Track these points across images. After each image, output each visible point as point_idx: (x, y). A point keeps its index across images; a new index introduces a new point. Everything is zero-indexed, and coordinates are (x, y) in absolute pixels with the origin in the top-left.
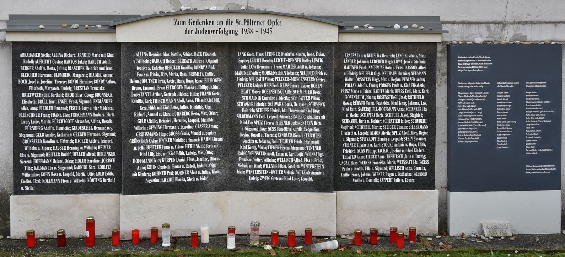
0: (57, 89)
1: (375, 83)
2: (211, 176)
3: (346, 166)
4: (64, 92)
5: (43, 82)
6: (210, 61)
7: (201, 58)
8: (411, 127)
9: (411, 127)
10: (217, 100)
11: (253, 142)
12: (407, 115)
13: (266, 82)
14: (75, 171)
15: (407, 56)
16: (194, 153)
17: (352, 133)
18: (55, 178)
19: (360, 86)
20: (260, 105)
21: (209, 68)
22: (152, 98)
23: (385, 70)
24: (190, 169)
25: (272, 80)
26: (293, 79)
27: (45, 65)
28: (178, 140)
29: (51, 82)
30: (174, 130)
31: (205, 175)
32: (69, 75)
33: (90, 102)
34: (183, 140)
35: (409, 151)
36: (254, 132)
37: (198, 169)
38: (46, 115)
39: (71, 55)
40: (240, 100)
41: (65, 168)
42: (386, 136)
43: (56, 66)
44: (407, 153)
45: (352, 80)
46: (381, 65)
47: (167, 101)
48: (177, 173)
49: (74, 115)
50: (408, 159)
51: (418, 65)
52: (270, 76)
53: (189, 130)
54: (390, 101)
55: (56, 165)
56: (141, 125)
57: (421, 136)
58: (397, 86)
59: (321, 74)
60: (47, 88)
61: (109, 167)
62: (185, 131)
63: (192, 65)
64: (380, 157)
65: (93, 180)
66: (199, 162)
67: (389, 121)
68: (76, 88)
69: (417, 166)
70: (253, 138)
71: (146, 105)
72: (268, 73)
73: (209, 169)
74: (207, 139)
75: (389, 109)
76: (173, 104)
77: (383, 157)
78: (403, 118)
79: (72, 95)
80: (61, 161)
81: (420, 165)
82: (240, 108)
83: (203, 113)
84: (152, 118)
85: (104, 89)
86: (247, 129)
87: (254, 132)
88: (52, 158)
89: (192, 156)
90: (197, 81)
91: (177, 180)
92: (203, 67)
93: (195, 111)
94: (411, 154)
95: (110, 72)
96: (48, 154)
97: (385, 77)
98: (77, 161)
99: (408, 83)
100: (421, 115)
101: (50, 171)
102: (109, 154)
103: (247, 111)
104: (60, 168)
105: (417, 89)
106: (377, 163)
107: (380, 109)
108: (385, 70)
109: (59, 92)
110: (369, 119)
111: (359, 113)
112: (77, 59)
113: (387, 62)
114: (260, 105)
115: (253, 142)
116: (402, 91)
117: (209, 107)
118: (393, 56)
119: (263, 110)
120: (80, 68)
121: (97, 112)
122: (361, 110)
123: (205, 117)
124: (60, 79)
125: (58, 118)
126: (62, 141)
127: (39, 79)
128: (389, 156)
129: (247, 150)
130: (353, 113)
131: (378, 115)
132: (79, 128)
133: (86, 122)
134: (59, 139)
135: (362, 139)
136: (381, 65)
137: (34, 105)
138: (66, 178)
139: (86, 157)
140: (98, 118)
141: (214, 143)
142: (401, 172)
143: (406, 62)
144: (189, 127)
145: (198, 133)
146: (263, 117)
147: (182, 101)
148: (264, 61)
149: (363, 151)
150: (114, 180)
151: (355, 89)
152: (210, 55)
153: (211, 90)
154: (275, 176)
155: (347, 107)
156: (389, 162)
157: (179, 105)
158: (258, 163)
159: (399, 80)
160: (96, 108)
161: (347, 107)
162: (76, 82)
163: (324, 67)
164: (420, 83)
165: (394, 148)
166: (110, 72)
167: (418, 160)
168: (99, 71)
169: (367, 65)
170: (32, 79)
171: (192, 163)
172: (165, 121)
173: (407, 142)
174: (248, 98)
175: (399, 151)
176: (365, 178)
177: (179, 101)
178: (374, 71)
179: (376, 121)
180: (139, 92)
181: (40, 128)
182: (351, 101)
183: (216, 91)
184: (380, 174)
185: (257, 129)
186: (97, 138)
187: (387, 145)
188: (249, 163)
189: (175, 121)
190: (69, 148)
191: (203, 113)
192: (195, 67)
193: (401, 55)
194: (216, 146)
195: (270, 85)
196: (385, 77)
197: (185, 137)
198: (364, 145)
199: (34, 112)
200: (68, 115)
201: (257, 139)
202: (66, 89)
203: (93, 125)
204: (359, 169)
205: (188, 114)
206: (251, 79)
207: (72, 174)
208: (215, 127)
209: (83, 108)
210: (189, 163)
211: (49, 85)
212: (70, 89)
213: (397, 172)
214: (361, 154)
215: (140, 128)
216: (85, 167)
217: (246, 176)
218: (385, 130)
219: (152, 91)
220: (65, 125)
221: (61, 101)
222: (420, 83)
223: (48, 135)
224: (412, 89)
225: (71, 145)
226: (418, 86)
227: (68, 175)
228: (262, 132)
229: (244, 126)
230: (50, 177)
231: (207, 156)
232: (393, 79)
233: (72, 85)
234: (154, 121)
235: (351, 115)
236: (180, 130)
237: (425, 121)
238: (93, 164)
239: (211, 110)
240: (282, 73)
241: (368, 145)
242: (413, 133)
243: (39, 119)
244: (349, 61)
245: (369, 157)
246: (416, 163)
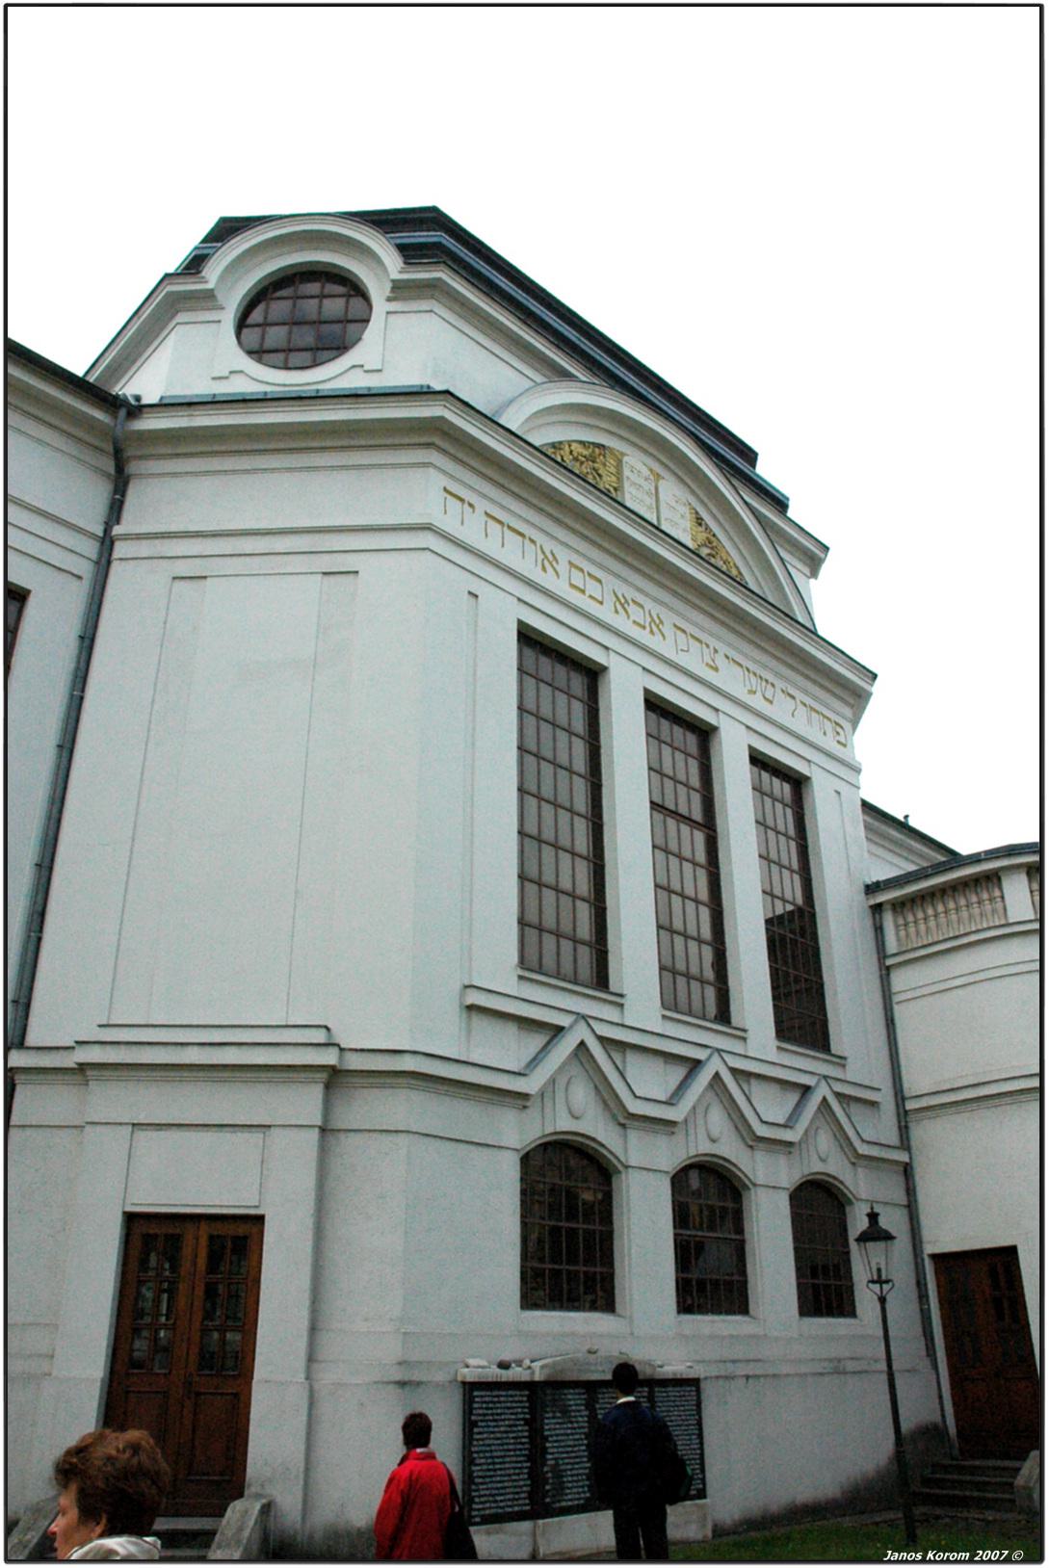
112: (506, 1396)
233: (504, 1420)
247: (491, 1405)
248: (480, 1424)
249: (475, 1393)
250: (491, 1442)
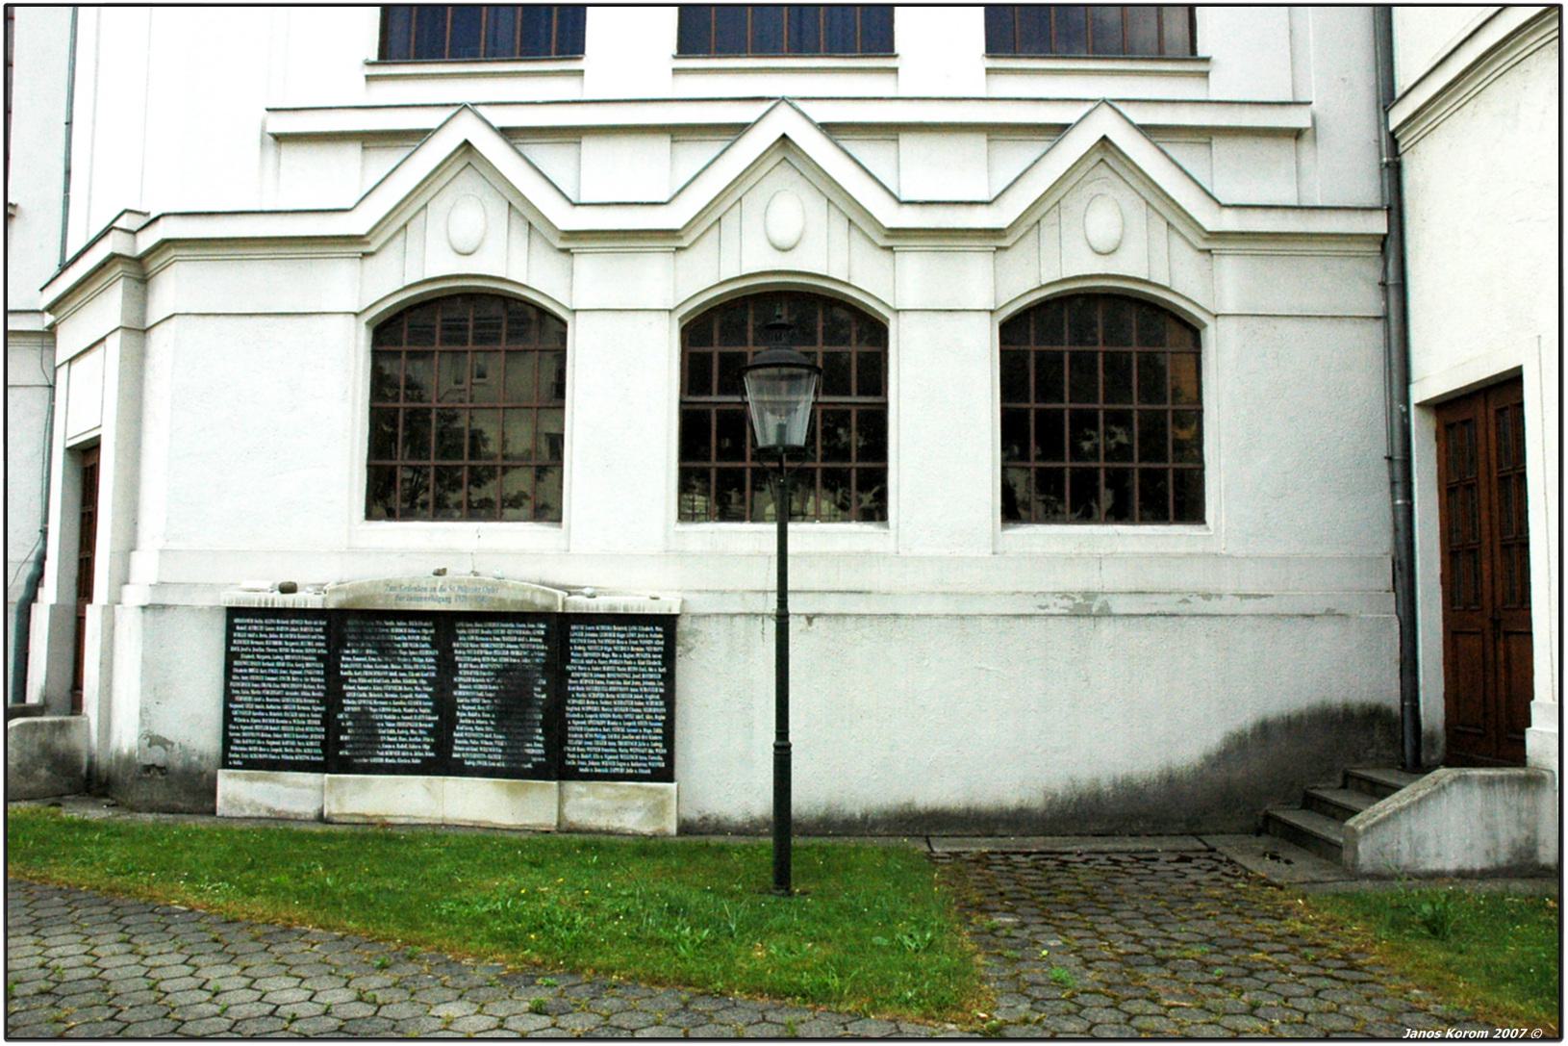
0: (269, 657)
1: (604, 659)
3: (571, 753)
4: (276, 661)
5: (254, 650)
6: (425, 631)
7: (415, 628)
8: (645, 710)
9: (645, 710)
10: (433, 674)
11: (469, 722)
12: (641, 697)
13: (484, 655)
14: (283, 747)
15: (643, 629)
16: (407, 732)
17: (578, 716)
18: (262, 753)
19: (588, 662)
20: (478, 680)
21: (425, 638)
22: (362, 670)
23: (616, 645)
24: (402, 750)
25: (490, 653)
26: (513, 653)
27: (257, 632)
28: (389, 717)
29: (262, 650)
30: (385, 706)
31: (419, 758)
32: (280, 643)
33: (300, 672)
34: (394, 717)
35: (643, 737)
36: (471, 711)
37: (409, 750)
38: (256, 685)
39: (283, 622)
40: (458, 675)
41: (273, 743)
42: (618, 720)
43: (268, 633)
44: (641, 740)
45: (578, 655)
46: (613, 638)
47: (379, 673)
48: (387, 753)
49: (284, 686)
50: (642, 747)
51: (655, 639)
52: (489, 649)
53: (401, 707)
54: (621, 680)
55: (265, 739)
56: (350, 699)
57: (657, 721)
58: (630, 663)
59: (543, 647)
60: (258, 657)
61: (318, 744)
62: (397, 707)
63: (406, 635)
64: (610, 744)
65: (301, 758)
66: (411, 743)
67: (621, 703)
68: (287, 657)
69: (652, 755)
70: (471, 718)
71: (356, 677)
72: (487, 646)
73: (423, 751)
74: (420, 717)
75: (621, 689)
76: (385, 677)
77: (614, 744)
78: (637, 700)
79: (283, 665)
80: (269, 736)
81: (656, 754)
83: (417, 688)
84: (361, 692)
85: (314, 659)
86: (464, 707)
87: (471, 711)
88: (260, 731)
89: (403, 736)
90: (412, 653)
91: (387, 760)
92: (418, 638)
93: (408, 685)
94: (646, 741)
95: (322, 641)
96: (257, 727)
97: (616, 652)
98: (285, 735)
99: (642, 659)
100: (658, 697)
101: (258, 746)
102: (318, 729)
103: (465, 687)
104: (268, 742)
105: (653, 667)
106: (606, 750)
107: (611, 689)
108: (616, 645)
109: (270, 661)
110: (598, 699)
112: (290, 626)
113: (618, 635)
114: (478, 680)
115: (469, 722)
116: (635, 669)
117: (423, 682)
118: (625, 629)
119: (481, 687)
120: (291, 636)
121: (307, 683)
122: (588, 689)
123: (419, 693)
124: (272, 647)
125: (269, 689)
126: (271, 714)
127: (251, 646)
128: (620, 743)
129: (464, 731)
130: (580, 692)
131: (608, 696)
132: (288, 700)
133: (296, 693)
134: (268, 711)
135: (590, 722)
136: (613, 638)
137: (245, 674)
138: (274, 753)
139: (295, 732)
140: (310, 691)
141: (428, 722)
142: (634, 761)
143: (639, 636)
144: (402, 703)
145: (411, 711)
146: (481, 694)
147: (395, 674)
148: (483, 632)
149: (591, 736)
150: (322, 759)
151: (582, 665)
152: (426, 624)
153: (426, 664)
154: (492, 761)
155: (573, 685)
156: (620, 750)
157: (390, 678)
158: (475, 746)
159: (632, 656)
160: (307, 680)
161: (573, 685)
162: (287, 650)
163: (546, 639)
164: (657, 660)
165: (626, 734)
166: (322, 641)
167: (654, 748)
168: (311, 640)
169: (596, 638)
170: (244, 646)
171: (404, 743)
172: (375, 695)
173: (642, 727)
174: (466, 673)
175: (632, 737)
176: (593, 767)
177: (391, 674)
178: (604, 645)
179: (606, 703)
180: (349, 663)
181: (250, 699)
182: (578, 679)
183: (431, 664)
184: (610, 764)
185: (474, 708)
186: (306, 712)
187: (618, 730)
188: (465, 746)
189: (387, 696)
190: (278, 721)
191: (417, 688)
192: (409, 638)
193: (635, 628)
194: (431, 725)
195: (488, 659)
196: (617, 652)
197: (397, 714)
198: (592, 729)
199: (244, 681)
200: (278, 686)
201: (474, 719)
202: (278, 657)
203: (303, 697)
204: (586, 757)
205: (400, 688)
206: (469, 652)
207: (280, 750)
208: (431, 704)
209: (294, 679)
210: (401, 743)
211: (262, 654)
212: (281, 658)
213: (629, 761)
214: (588, 740)
215: (348, 702)
216: (293, 743)
217: (462, 760)
218: (617, 713)
219: (362, 663)
220: (275, 696)
221: (272, 671)
222: (657, 660)
223: (258, 707)
224: (647, 666)
225: (280, 718)
226: (655, 663)
227: (276, 750)
228: (480, 712)
229: (461, 704)
230: (258, 752)
232: (625, 656)
233: (283, 654)
234: (364, 695)
235: (578, 695)
236: (392, 706)
237: (661, 703)
238: (301, 740)
239: (426, 685)
240: (502, 645)
241: (597, 729)
242: (648, 717)
243: (249, 689)
244: (576, 634)
245: (597, 743)
246: (651, 751)
247: (261, 636)
248: (242, 656)
249: (237, 621)
250: (262, 678)
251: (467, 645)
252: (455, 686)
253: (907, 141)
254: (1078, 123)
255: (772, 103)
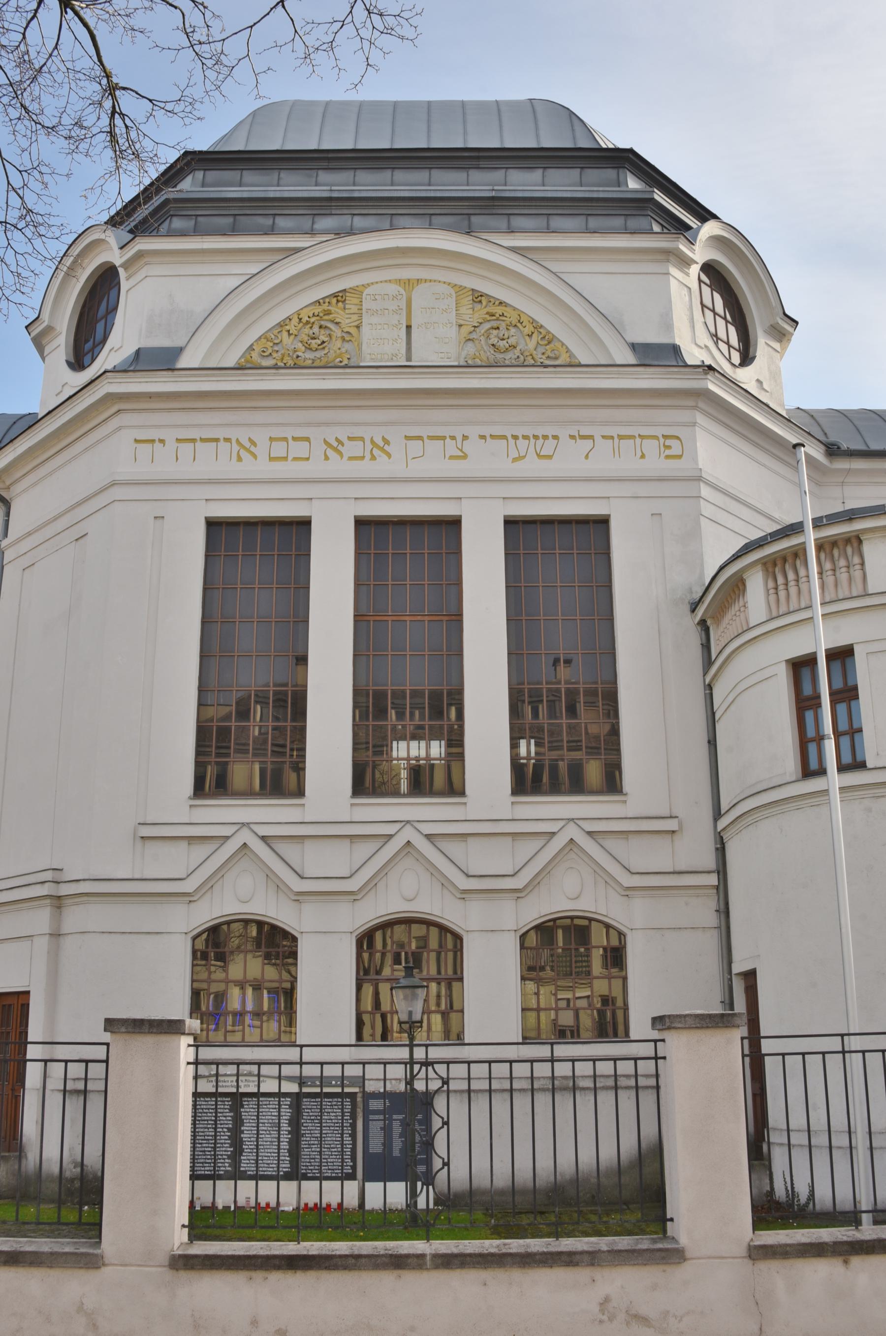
2: (226, 1171)
6: (227, 1103)
10: (231, 1126)
19: (312, 1118)
21: (226, 1107)
26: (273, 1114)
40: (243, 1126)
42: (327, 1148)
47: (202, 1126)
54: (329, 1127)
59: (288, 1110)
67: (329, 1139)
70: (250, 1149)
73: (225, 1167)
74: (224, 1149)
76: (205, 1128)
82: (243, 1131)
83: (222, 1134)
91: (206, 1173)
92: (222, 1107)
111: (311, 1134)
116: (336, 1121)
117: (225, 1130)
122: (312, 1132)
128: (329, 1160)
135: (313, 1149)
141: (228, 1151)
157: (208, 1128)
163: (290, 1107)
165: (332, 1155)
174: (248, 1125)
176: (315, 1173)
177: (209, 1126)
182: (307, 1127)
188: (247, 1164)
189: (206, 1138)
191: (222, 1134)
193: (336, 1100)
194: (229, 1153)
206: (250, 1114)
208: (229, 1142)
213: (333, 1170)
217: (246, 1171)
231: (224, 1159)
237: (350, 1139)
240: (267, 1110)
251: (248, 1110)
252: (242, 1132)
253: (470, 840)
254: (559, 831)
255: (403, 823)
